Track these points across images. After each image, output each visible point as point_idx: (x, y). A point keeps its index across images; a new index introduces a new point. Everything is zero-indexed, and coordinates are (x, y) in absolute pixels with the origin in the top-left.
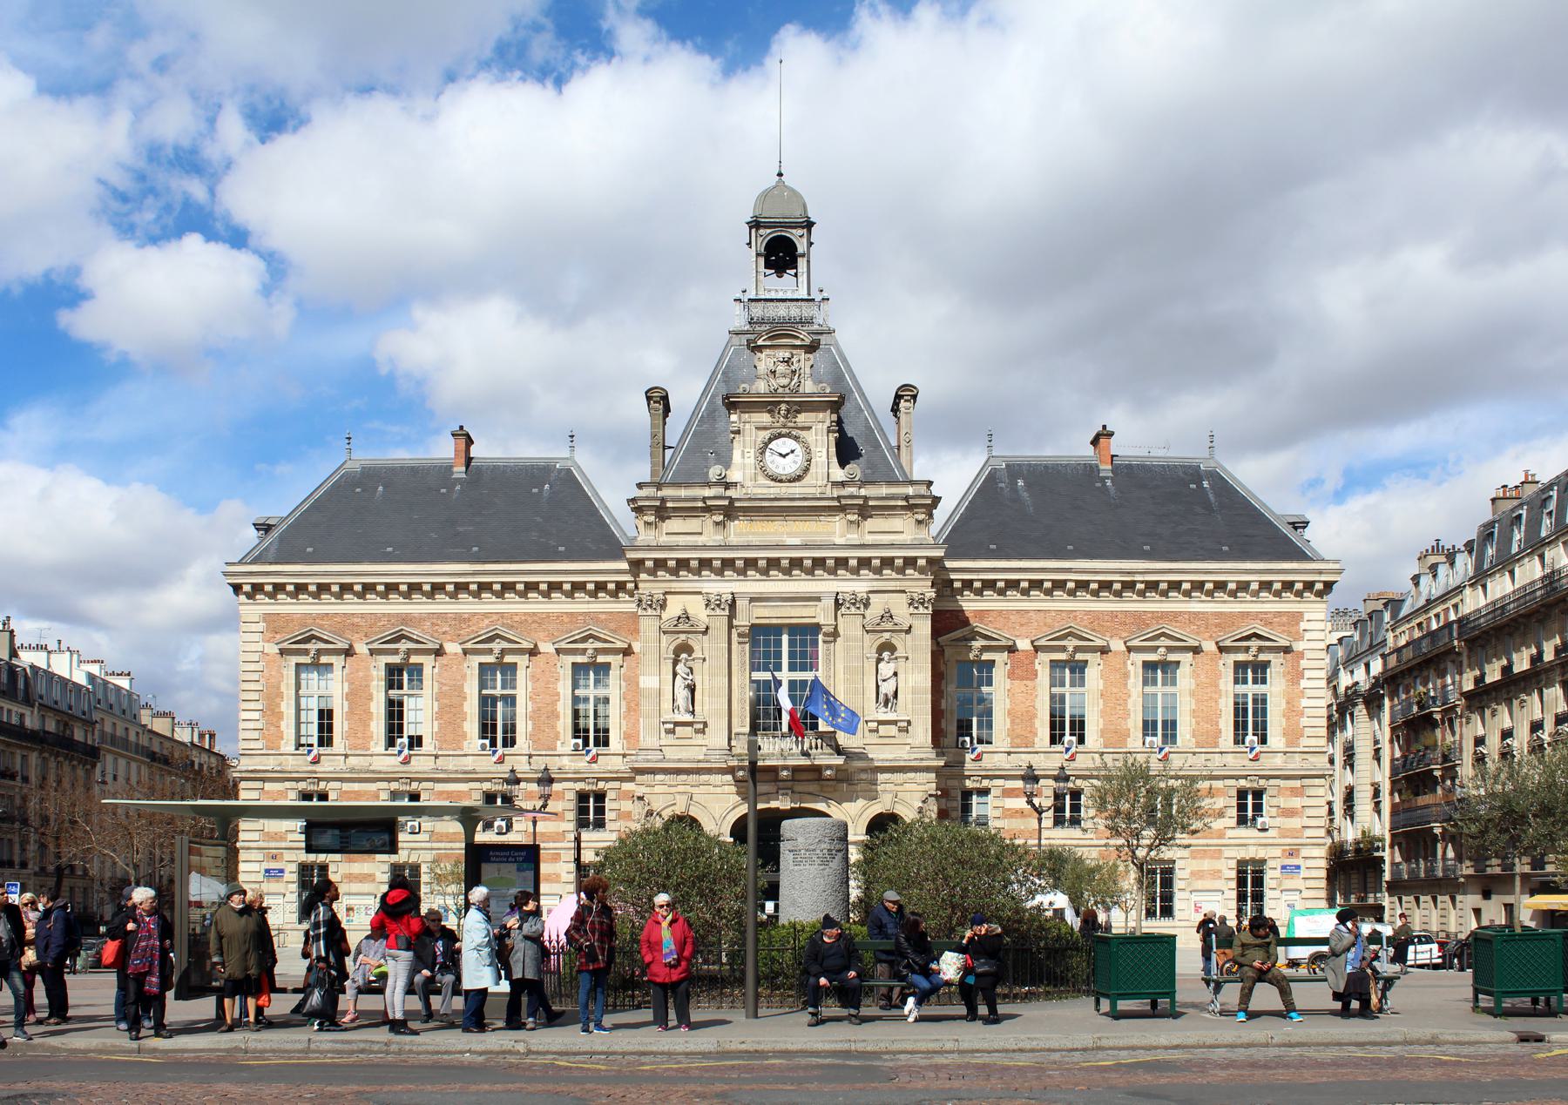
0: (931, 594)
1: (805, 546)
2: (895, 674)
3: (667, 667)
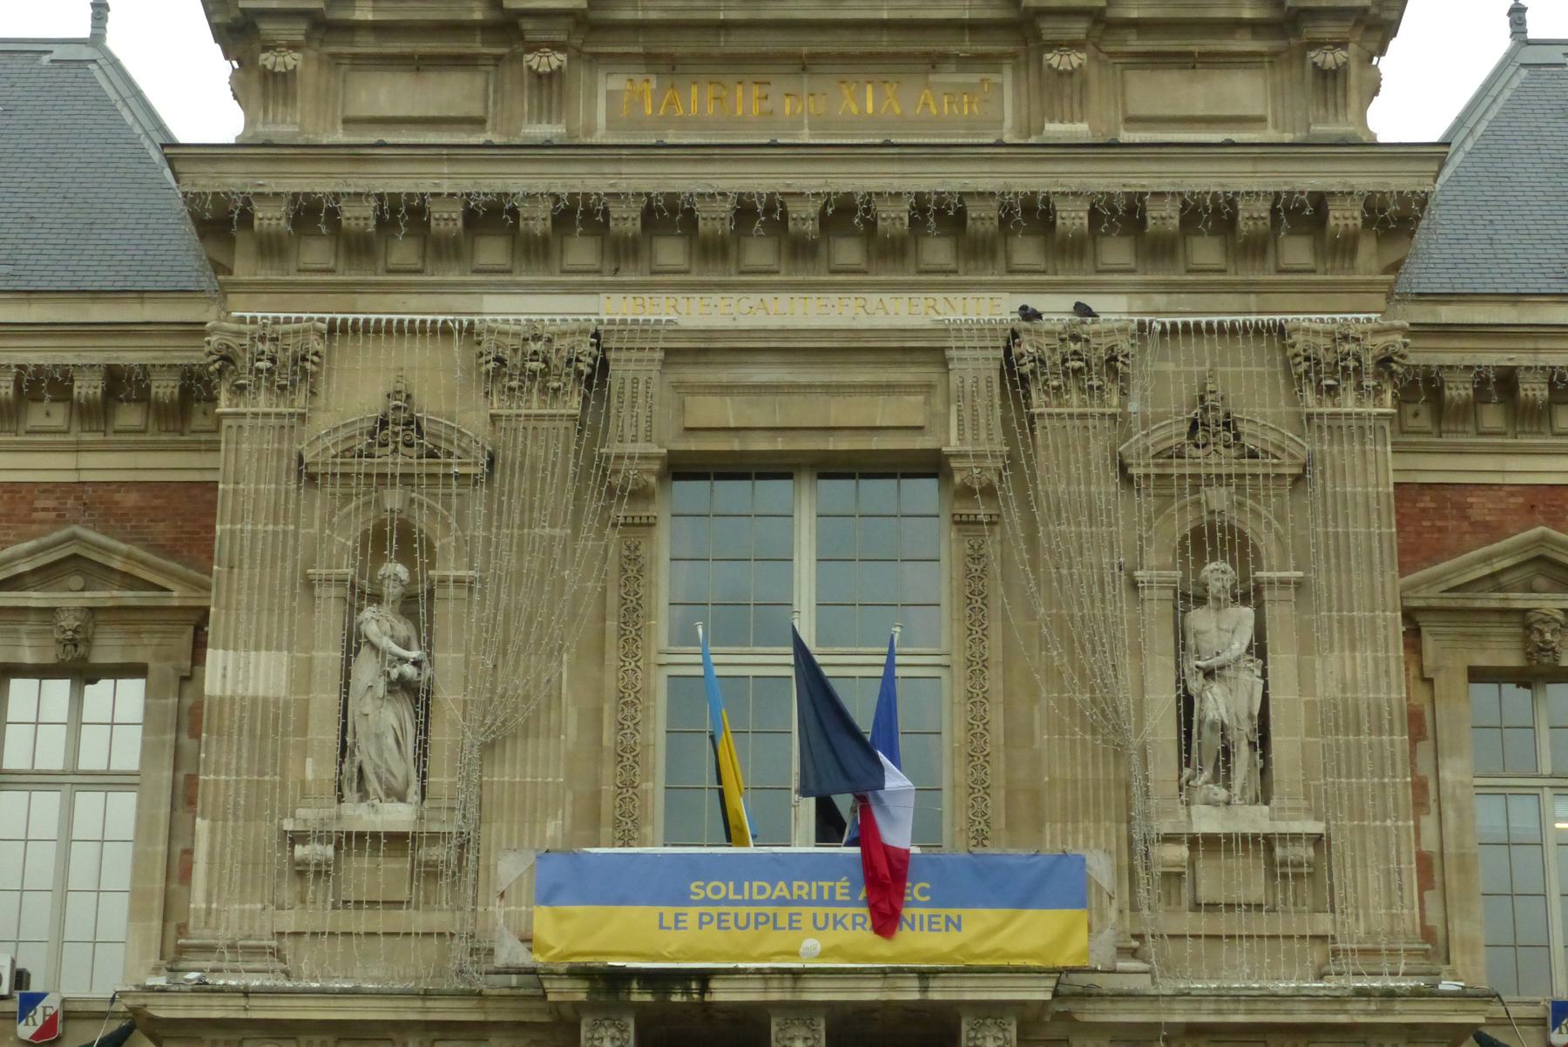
1: (887, 151)
3: (329, 615)
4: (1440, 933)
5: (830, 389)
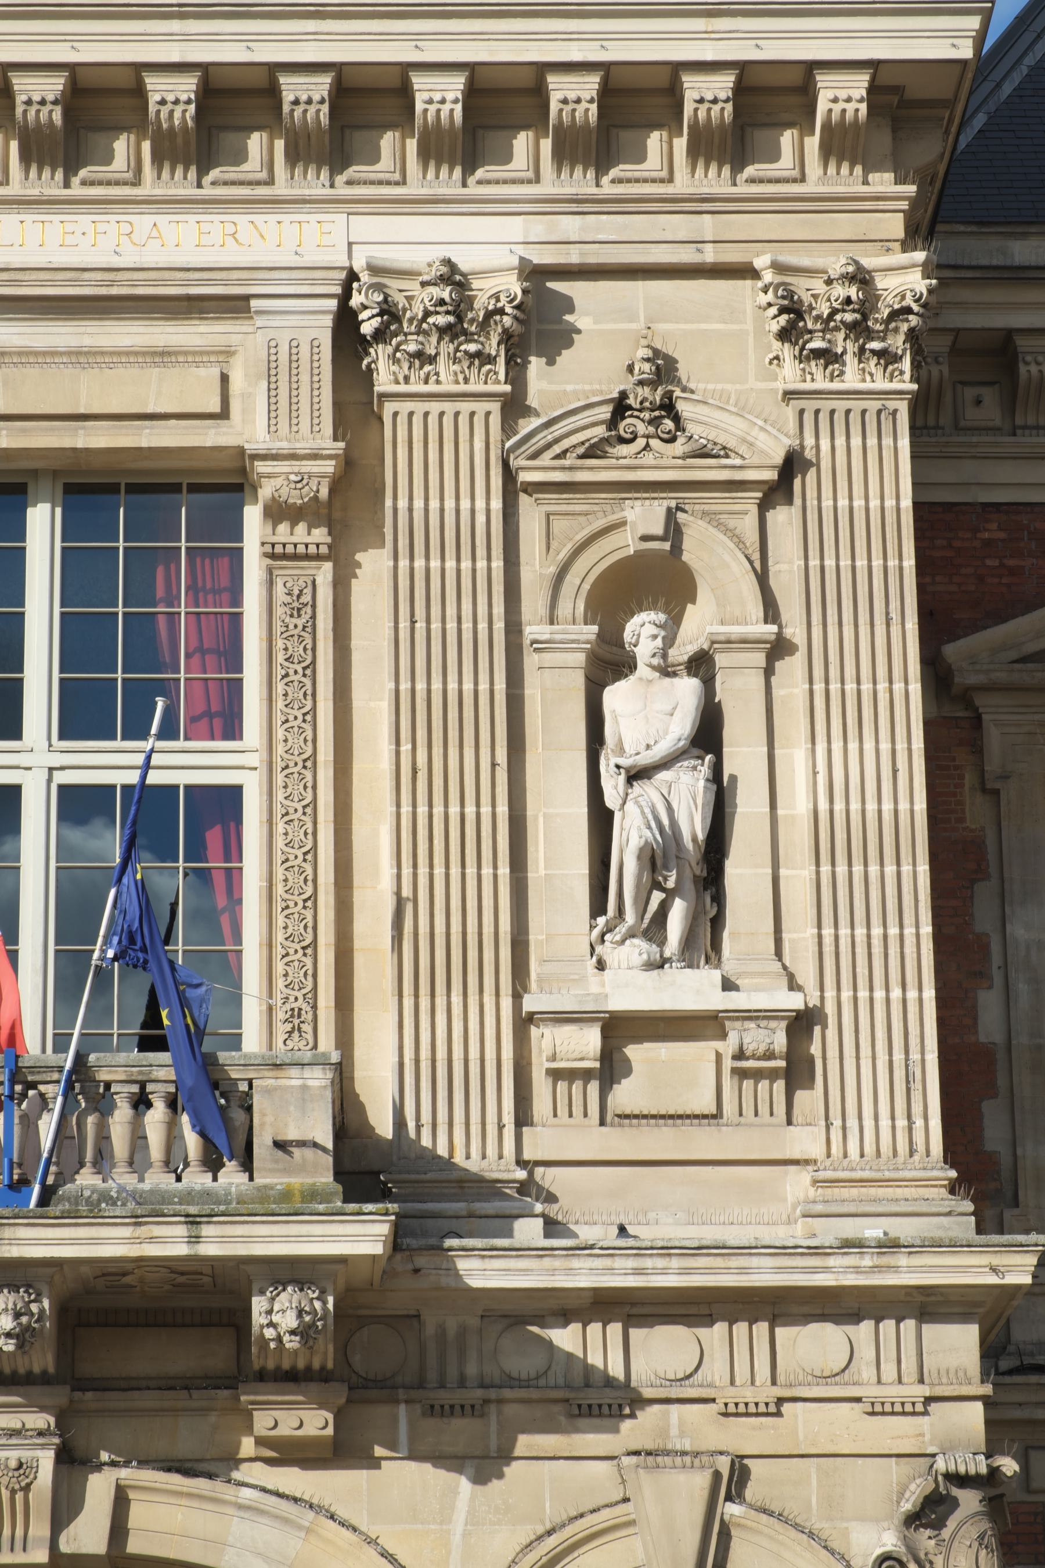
0: (904, 278)
2: (708, 735)
4: (1005, 1160)
5: (81, 357)
